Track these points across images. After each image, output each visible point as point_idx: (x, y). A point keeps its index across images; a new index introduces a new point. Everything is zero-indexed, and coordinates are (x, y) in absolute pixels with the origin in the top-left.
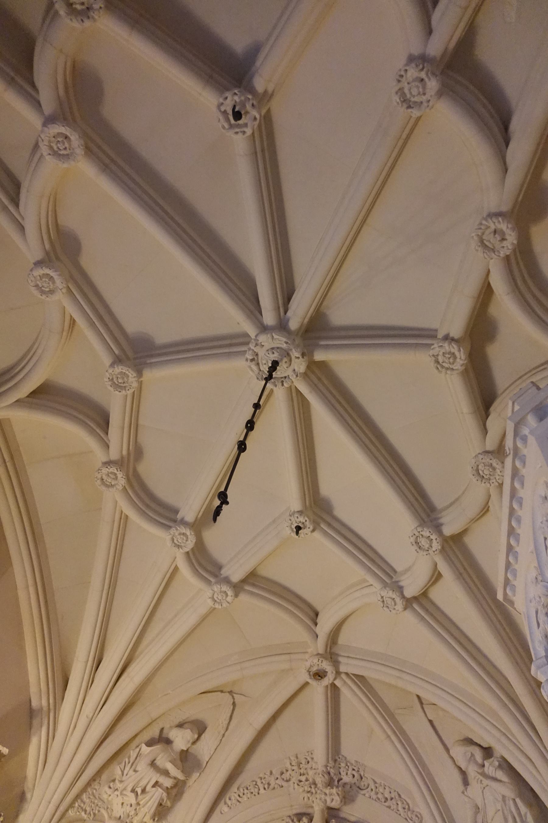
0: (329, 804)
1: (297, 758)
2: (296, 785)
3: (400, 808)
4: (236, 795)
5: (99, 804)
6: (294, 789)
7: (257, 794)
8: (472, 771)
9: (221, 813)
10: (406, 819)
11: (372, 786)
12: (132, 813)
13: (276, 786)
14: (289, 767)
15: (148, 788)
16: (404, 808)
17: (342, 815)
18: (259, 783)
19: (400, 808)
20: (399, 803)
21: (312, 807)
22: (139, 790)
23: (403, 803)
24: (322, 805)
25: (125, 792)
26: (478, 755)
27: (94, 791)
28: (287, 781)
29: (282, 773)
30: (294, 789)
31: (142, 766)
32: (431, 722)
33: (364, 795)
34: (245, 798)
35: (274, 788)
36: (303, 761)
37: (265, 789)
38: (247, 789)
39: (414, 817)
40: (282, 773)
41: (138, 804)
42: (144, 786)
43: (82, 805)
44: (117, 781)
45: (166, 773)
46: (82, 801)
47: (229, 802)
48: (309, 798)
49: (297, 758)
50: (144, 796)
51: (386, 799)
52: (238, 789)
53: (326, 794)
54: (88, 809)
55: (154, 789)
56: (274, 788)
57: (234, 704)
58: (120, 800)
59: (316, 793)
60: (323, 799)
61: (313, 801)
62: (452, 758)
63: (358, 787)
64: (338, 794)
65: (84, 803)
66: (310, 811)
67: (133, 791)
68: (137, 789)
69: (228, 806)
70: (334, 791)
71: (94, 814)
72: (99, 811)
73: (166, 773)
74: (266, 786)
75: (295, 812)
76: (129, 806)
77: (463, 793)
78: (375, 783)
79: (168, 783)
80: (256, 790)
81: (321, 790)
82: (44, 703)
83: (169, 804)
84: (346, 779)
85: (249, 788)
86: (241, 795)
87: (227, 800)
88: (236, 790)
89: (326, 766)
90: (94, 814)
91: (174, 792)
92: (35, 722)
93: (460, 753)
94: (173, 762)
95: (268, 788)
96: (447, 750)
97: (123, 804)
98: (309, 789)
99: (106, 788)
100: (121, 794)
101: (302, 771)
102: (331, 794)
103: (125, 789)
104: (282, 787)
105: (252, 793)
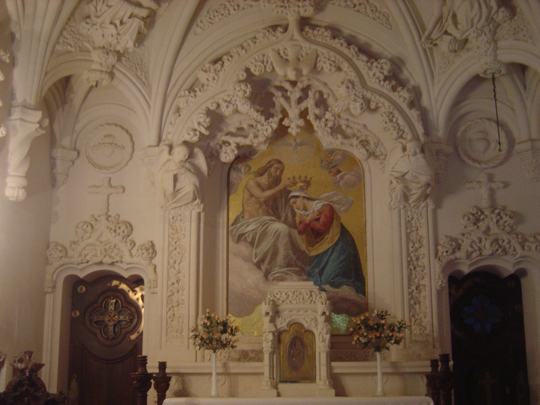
0: (303, 14)
2: (267, 4)
4: (207, 18)
5: (81, 38)
6: (265, 6)
7: (227, 15)
9: (195, 34)
10: (374, 19)
12: (115, 41)
13: (246, 7)
15: (125, 19)
16: (372, 11)
17: (314, 22)
18: (228, 5)
19: (368, 10)
20: (368, 7)
21: (287, 19)
22: (118, 22)
23: (371, 7)
24: (296, 16)
25: (103, 25)
27: (72, 28)
30: (265, 6)
33: (334, 4)
34: (217, 19)
37: (235, 10)
38: (217, 12)
39: (381, 16)
41: (118, 34)
42: (121, 18)
43: (66, 40)
44: (92, 17)
46: (64, 37)
47: (202, 25)
48: (282, 12)
50: (123, 26)
51: (355, 6)
52: (208, 13)
53: (299, 6)
54: (72, 43)
55: (131, 20)
56: (244, 9)
59: (289, 6)
60: (296, 10)
61: (287, 14)
64: (310, 5)
65: (67, 39)
66: (284, 23)
67: (111, 23)
68: (114, 22)
69: (201, 28)
71: (79, 47)
72: (82, 44)
74: (236, 8)
75: (267, 25)
76: (110, 36)
79: (144, 13)
80: (227, 12)
81: (294, 4)
83: (146, 31)
85: (219, 11)
86: (212, 17)
87: (199, 23)
88: (206, 14)
90: (79, 47)
91: (148, 21)
95: (238, 8)
97: (103, 36)
98: (282, 4)
99: (84, 24)
100: (100, 26)
102: (303, 6)
103: (103, 23)
104: (252, 6)
105: (223, 15)
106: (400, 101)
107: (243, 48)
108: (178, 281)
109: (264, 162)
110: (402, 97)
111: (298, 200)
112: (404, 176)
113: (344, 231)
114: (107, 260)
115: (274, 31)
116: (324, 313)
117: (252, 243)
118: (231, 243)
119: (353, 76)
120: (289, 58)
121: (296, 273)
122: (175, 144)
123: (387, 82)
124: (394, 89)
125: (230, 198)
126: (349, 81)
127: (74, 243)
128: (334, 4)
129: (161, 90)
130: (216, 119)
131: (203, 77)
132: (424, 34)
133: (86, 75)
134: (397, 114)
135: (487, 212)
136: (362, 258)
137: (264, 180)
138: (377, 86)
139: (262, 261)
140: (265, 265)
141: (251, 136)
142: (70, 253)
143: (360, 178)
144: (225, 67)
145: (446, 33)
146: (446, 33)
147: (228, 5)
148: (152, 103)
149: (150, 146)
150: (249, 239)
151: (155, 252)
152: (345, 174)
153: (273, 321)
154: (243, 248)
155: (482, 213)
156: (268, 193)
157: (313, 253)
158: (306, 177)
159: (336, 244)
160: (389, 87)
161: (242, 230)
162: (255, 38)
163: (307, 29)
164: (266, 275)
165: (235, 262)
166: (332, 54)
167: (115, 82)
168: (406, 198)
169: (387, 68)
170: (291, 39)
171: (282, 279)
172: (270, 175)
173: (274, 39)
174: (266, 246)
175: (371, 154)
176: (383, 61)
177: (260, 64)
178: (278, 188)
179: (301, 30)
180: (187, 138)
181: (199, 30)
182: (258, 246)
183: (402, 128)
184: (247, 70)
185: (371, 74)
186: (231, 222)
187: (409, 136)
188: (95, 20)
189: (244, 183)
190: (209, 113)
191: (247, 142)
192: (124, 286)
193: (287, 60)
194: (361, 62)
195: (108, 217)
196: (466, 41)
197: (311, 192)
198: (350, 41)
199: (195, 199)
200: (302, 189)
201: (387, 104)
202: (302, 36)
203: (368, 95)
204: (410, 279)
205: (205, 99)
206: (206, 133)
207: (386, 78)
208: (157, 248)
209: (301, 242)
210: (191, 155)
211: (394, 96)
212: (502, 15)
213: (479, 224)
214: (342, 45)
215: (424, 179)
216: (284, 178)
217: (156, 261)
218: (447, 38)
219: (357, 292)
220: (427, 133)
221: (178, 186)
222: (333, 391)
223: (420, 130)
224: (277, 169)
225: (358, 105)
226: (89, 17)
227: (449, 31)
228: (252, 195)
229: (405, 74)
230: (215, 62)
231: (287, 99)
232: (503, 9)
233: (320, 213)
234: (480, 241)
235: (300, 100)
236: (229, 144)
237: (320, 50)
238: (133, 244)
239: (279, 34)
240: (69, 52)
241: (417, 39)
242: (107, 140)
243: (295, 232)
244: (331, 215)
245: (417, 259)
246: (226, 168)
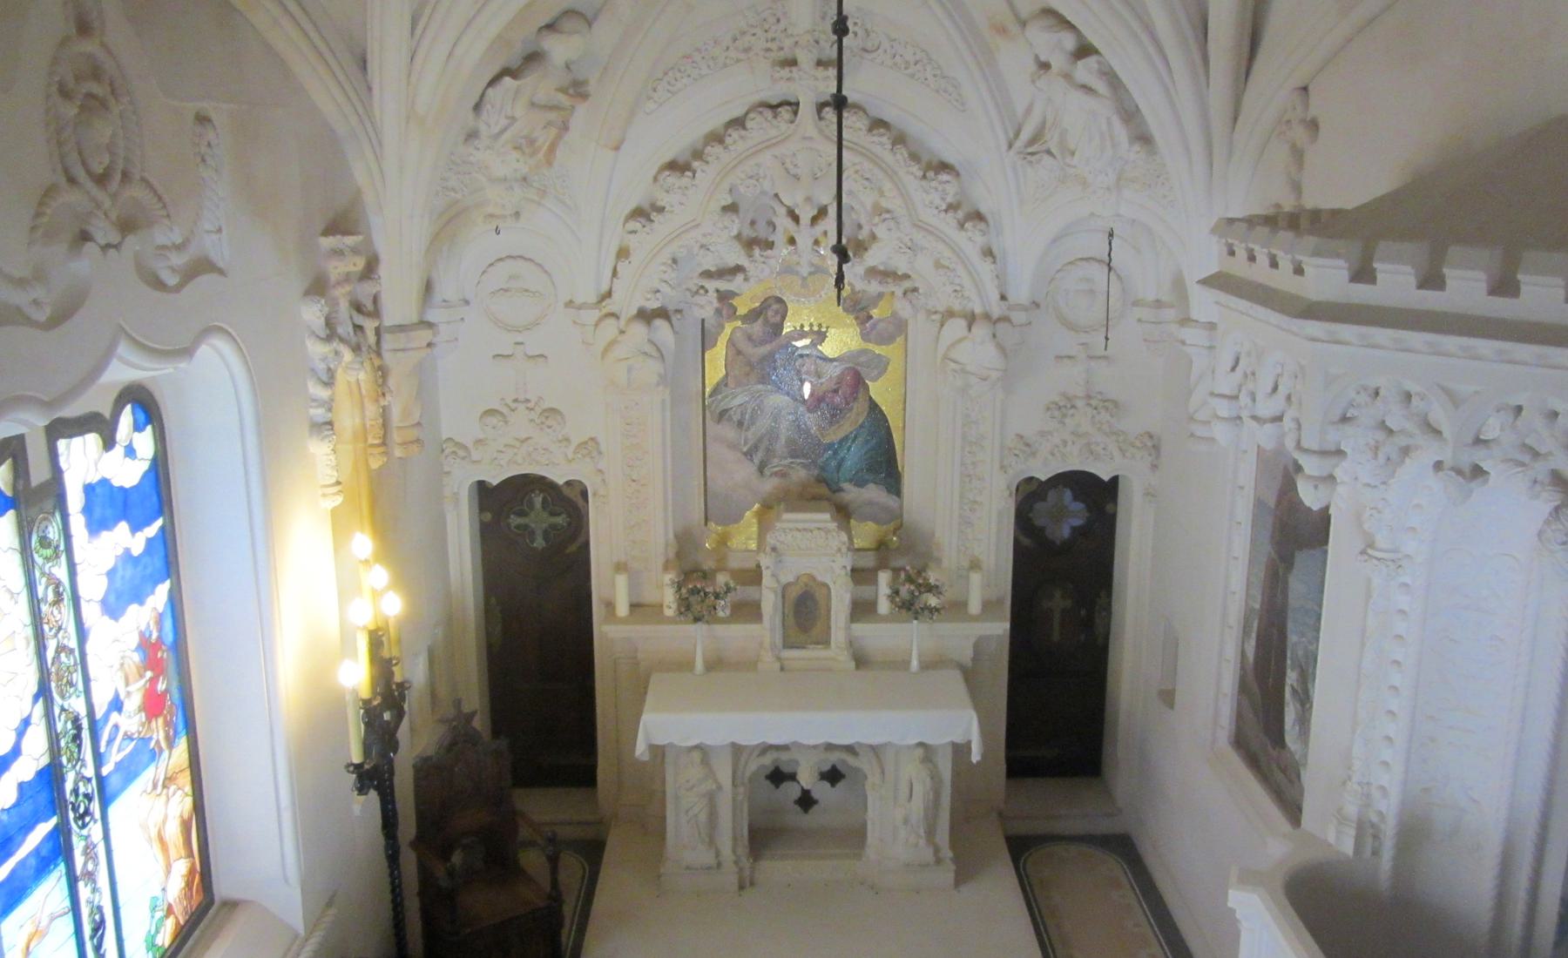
3: (929, 68)
11: (886, 45)
18: (697, 57)
28: (747, 50)
29: (735, 40)
35: (725, 66)
36: (772, 20)
39: (951, 89)
40: (735, 40)
51: (907, 62)
63: (865, 50)
101: (770, 35)
110: (970, 241)
113: (874, 407)
117: (740, 424)
121: (804, 466)
123: (950, 214)
127: (479, 442)
128: (872, 60)
132: (1017, 135)
134: (961, 271)
135: (1080, 403)
137: (757, 328)
139: (756, 447)
142: (475, 455)
144: (696, 182)
146: (1049, 152)
150: (736, 418)
152: (880, 320)
154: (728, 431)
155: (1073, 407)
157: (826, 441)
158: (820, 325)
159: (861, 426)
160: (954, 223)
161: (723, 406)
164: (761, 469)
165: (715, 450)
166: (867, 165)
172: (766, 320)
173: (773, 132)
177: (753, 181)
180: (642, 303)
182: (748, 429)
183: (966, 293)
193: (797, 177)
194: (910, 175)
197: (829, 348)
202: (821, 131)
204: (962, 496)
207: (952, 207)
208: (603, 447)
209: (811, 420)
212: (1135, 153)
213: (1067, 421)
214: (881, 144)
215: (994, 375)
218: (1047, 159)
219: (889, 491)
220: (1003, 298)
224: (777, 312)
227: (1054, 151)
228: (739, 353)
231: (796, 219)
232: (1137, 147)
233: (840, 380)
234: (1065, 443)
235: (814, 220)
238: (567, 440)
240: (457, 201)
243: (802, 409)
244: (855, 380)
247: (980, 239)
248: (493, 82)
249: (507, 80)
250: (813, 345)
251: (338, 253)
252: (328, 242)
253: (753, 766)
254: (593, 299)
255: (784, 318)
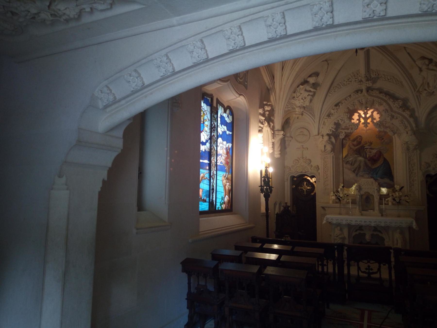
0: (368, 85)
1: (353, 73)
8: (424, 68)
14: (350, 77)
18: (340, 84)
26: (427, 62)
28: (351, 82)
31: (302, 92)
32: (408, 53)
45: (310, 91)
49: (353, 73)
51: (388, 80)
57: (328, 64)
58: (298, 102)
62: (417, 65)
67: (302, 99)
70: (370, 82)
73: (310, 91)
77: (419, 74)
78: (384, 75)
79: (311, 94)
82: (271, 86)
84: (372, 76)
89: (365, 75)
92: (270, 92)
93: (419, 63)
94: (311, 88)
96: (415, 62)
106: (406, 115)
107: (346, 100)
108: (327, 178)
109: (355, 137)
110: (407, 114)
111: (368, 150)
112: (407, 142)
113: (385, 159)
114: (304, 171)
115: (357, 92)
116: (377, 190)
117: (351, 164)
118: (345, 165)
119: (387, 107)
120: (363, 103)
122: (324, 135)
124: (404, 111)
125: (344, 149)
126: (386, 109)
127: (293, 166)
129: (318, 116)
130: (337, 125)
131: (332, 111)
133: (294, 116)
136: (392, 169)
138: (397, 110)
139: (355, 170)
140: (356, 171)
141: (350, 129)
143: (391, 141)
145: (425, 90)
146: (425, 90)
147: (340, 84)
148: (315, 121)
149: (316, 135)
150: (350, 163)
151: (319, 169)
153: (359, 192)
154: (349, 166)
156: (357, 147)
157: (373, 167)
161: (347, 160)
162: (350, 96)
163: (370, 91)
164: (357, 175)
166: (379, 100)
167: (303, 116)
168: (408, 149)
169: (401, 103)
170: (364, 96)
171: (363, 176)
174: (356, 165)
175: (394, 134)
176: (399, 101)
178: (360, 145)
179: (368, 91)
180: (328, 133)
181: (330, 95)
184: (348, 108)
185: (395, 106)
186: (344, 157)
187: (409, 128)
188: (296, 98)
189: (348, 144)
190: (335, 124)
191: (349, 131)
192: (309, 178)
193: (362, 104)
194: (391, 102)
195: (303, 158)
196: (433, 92)
198: (387, 94)
199: (331, 152)
200: (369, 145)
201: (401, 117)
203: (393, 114)
205: (333, 119)
206: (334, 130)
207: (401, 107)
209: (369, 164)
210: (330, 138)
211: (404, 114)
216: (362, 142)
217: (319, 171)
218: (425, 92)
220: (417, 126)
221: (326, 148)
222: (380, 215)
223: (414, 125)
225: (389, 118)
226: (294, 97)
228: (351, 148)
229: (409, 104)
230: (337, 105)
236: (342, 132)
237: (375, 99)
238: (312, 166)
239: (359, 94)
240: (289, 110)
241: (413, 91)
242: (301, 133)
244: (380, 154)
245: (413, 170)
246: (341, 140)
247: (409, 113)
248: (298, 86)
249: (301, 86)
250: (369, 145)
251: (266, 105)
252: (265, 103)
253: (354, 234)
254: (317, 133)
255: (362, 139)
